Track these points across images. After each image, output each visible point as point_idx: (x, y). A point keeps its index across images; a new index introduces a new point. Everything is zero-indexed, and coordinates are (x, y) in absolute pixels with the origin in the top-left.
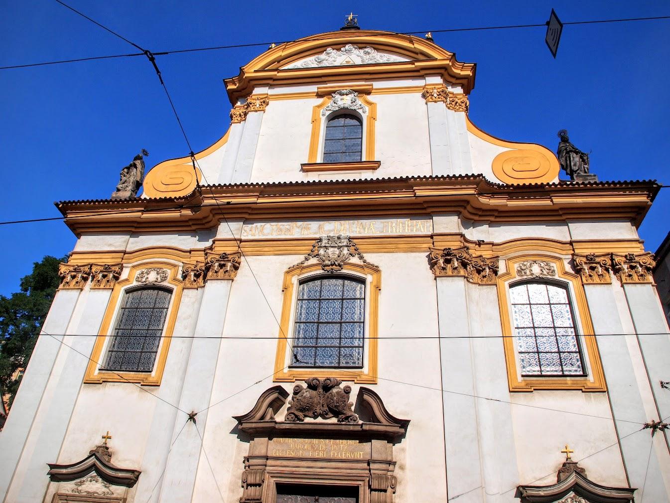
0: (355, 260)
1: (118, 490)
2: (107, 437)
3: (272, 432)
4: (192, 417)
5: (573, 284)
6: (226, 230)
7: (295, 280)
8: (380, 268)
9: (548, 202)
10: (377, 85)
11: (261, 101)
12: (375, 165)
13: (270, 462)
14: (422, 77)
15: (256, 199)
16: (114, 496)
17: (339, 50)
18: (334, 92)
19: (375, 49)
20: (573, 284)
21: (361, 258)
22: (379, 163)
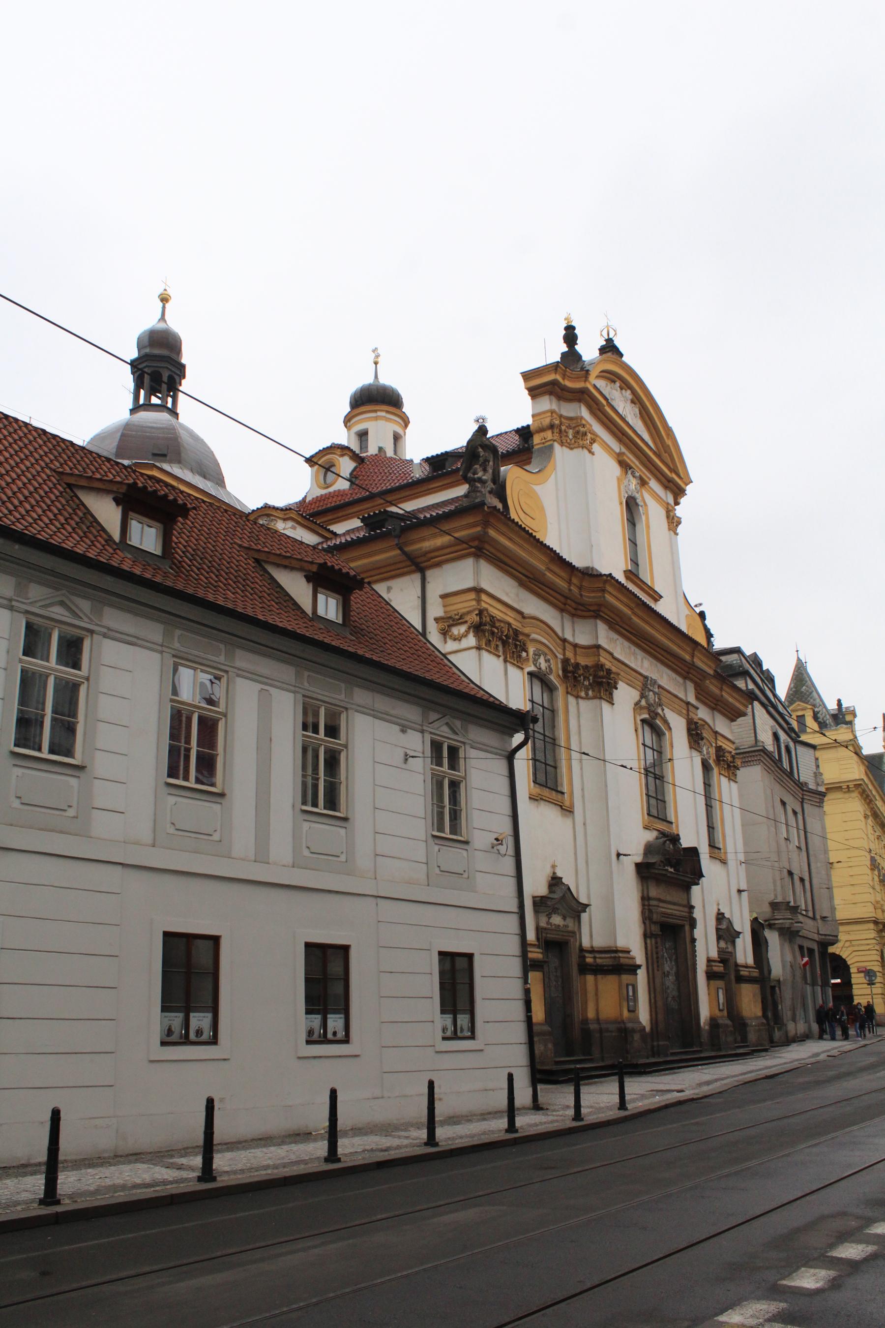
0: (660, 711)
1: (571, 924)
2: (554, 866)
3: (660, 879)
4: (618, 855)
5: (716, 771)
6: (604, 636)
7: (639, 718)
8: (671, 726)
9: (716, 691)
10: (653, 484)
11: (593, 437)
12: (657, 597)
13: (661, 904)
14: (666, 488)
15: (630, 613)
16: (570, 929)
17: (621, 389)
18: (631, 468)
19: (640, 413)
20: (716, 771)
21: (663, 710)
22: (661, 597)
